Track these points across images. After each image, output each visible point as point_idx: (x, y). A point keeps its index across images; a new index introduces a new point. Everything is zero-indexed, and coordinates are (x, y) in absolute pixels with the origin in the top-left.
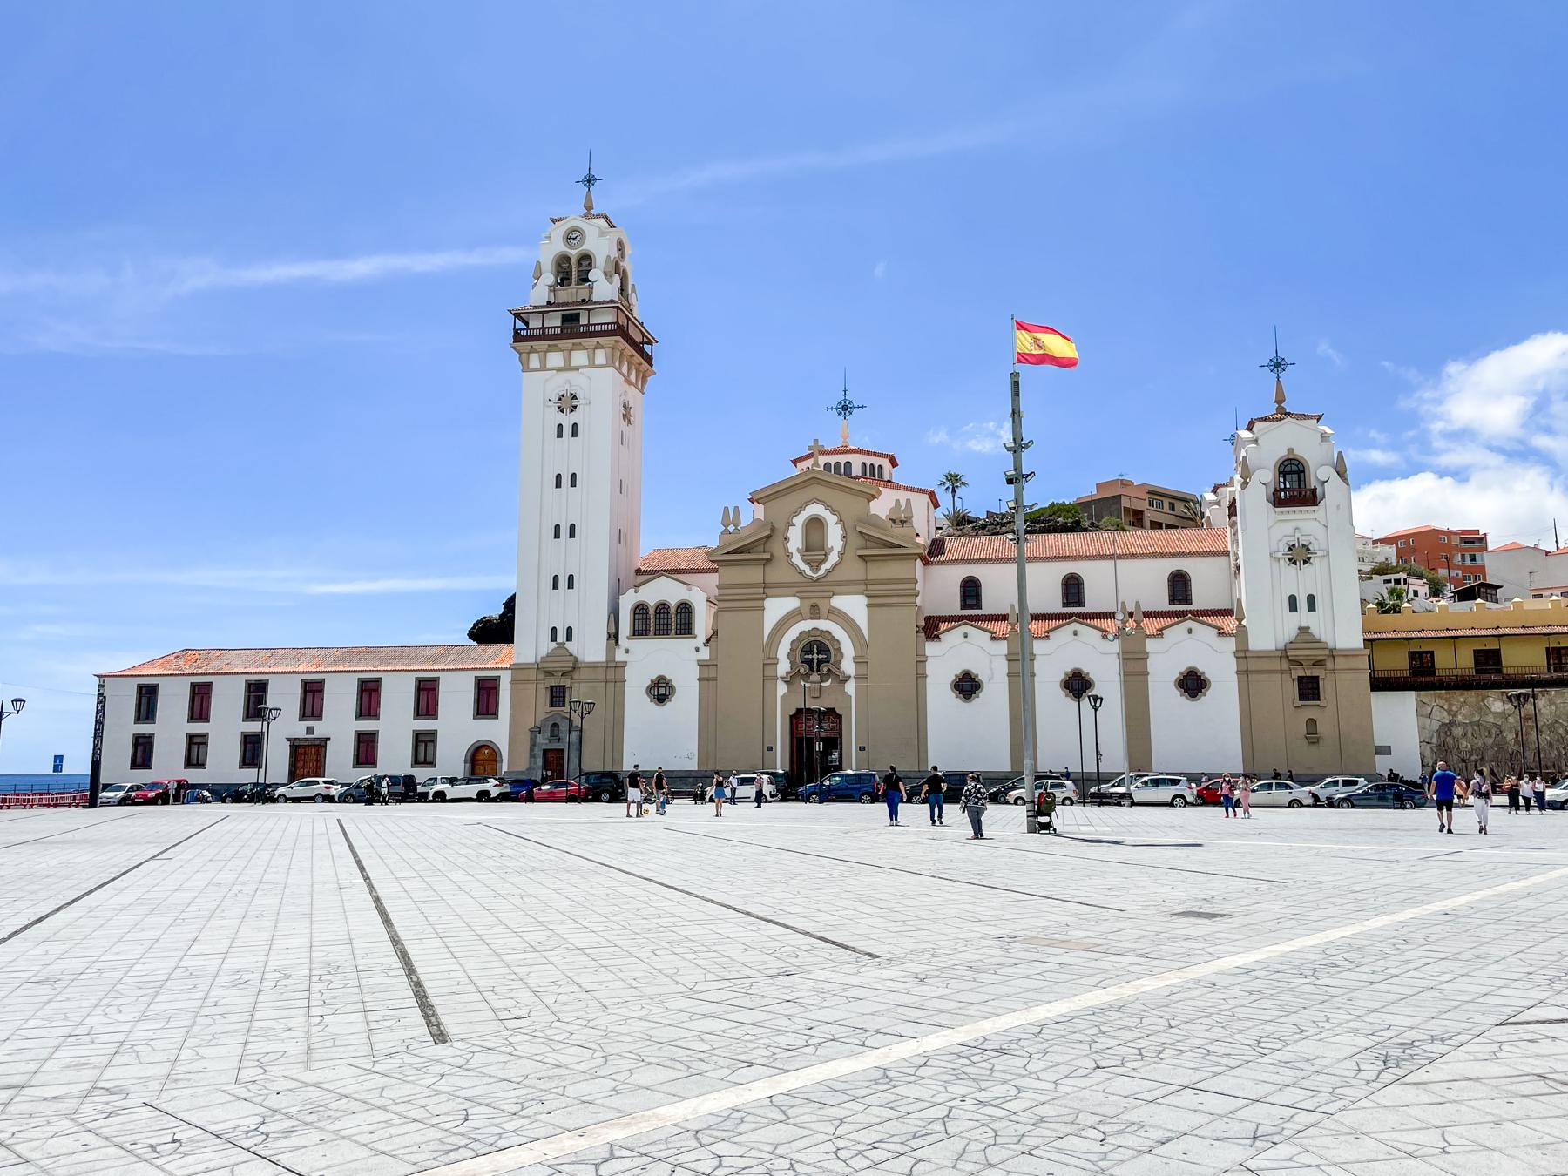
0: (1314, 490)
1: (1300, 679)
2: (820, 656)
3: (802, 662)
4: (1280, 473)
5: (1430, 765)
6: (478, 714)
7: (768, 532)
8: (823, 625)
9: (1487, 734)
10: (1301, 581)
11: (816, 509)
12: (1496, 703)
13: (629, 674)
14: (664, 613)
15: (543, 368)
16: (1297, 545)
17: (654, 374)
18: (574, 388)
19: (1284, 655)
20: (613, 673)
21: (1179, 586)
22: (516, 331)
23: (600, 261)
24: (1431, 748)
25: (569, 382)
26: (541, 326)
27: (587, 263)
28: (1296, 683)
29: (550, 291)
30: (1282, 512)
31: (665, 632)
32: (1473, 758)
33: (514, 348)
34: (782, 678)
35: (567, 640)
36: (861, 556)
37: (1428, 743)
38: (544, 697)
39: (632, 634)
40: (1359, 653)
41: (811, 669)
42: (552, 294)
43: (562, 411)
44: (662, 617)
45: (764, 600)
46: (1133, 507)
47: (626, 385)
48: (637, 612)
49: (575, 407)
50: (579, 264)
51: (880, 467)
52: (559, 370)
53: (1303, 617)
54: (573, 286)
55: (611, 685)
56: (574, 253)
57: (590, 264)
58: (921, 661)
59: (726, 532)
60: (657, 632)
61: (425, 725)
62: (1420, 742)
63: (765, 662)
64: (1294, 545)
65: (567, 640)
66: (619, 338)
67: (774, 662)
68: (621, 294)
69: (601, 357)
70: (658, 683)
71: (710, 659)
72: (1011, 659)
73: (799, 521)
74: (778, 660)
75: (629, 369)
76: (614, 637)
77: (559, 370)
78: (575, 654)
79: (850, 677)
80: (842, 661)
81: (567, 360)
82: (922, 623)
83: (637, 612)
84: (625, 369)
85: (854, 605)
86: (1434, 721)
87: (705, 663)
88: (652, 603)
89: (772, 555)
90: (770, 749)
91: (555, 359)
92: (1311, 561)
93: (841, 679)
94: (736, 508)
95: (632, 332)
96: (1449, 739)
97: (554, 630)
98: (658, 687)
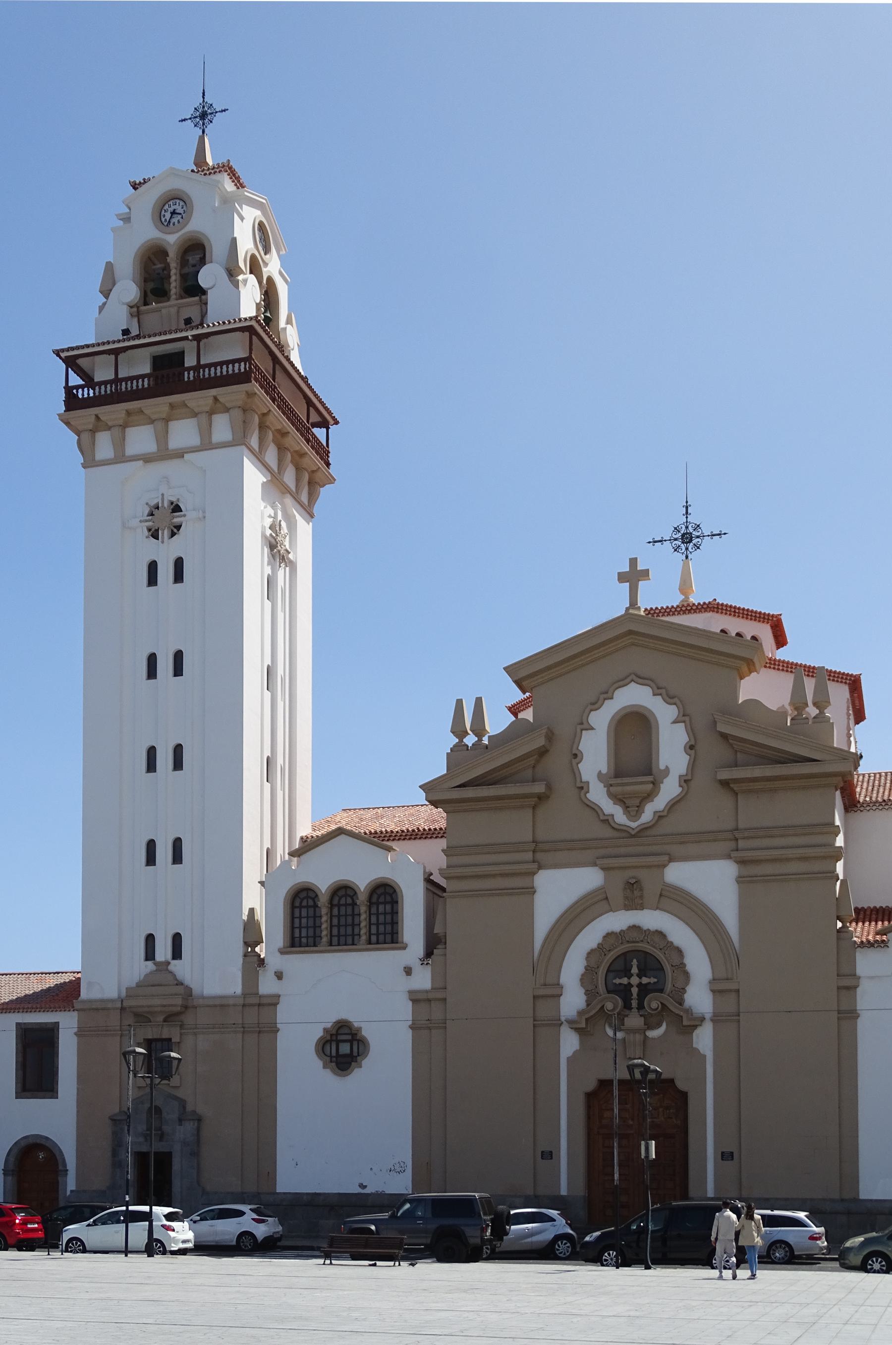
2: (645, 980)
3: (609, 992)
22: (69, 390)
26: (113, 377)
31: (350, 940)
34: (570, 1022)
41: (627, 1006)
42: (136, 320)
44: (343, 912)
45: (534, 874)
50: (183, 262)
54: (173, 302)
67: (555, 992)
69: (222, 427)
70: (337, 1034)
79: (703, 1019)
83: (297, 904)
88: (323, 884)
93: (685, 1023)
94: (479, 701)
98: (338, 1042)
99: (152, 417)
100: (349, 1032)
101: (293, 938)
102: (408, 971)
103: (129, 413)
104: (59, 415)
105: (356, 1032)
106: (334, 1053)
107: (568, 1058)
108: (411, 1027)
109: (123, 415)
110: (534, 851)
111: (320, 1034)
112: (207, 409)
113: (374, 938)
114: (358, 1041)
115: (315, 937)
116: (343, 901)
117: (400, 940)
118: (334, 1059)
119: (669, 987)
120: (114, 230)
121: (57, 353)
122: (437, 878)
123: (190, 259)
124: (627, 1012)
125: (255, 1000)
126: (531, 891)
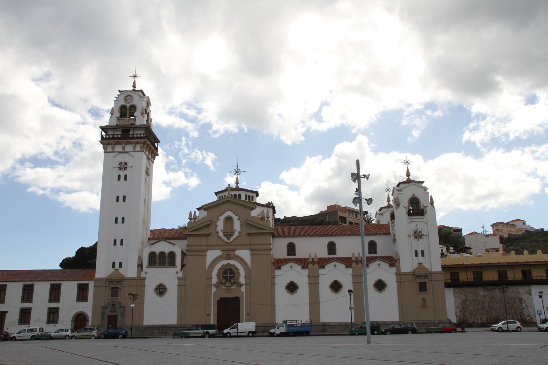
0: (423, 210)
1: (420, 283)
2: (231, 275)
3: (223, 278)
4: (410, 203)
5: (459, 316)
6: (78, 300)
7: (209, 223)
8: (232, 262)
9: (478, 304)
10: (420, 245)
11: (229, 214)
12: (481, 292)
13: (147, 283)
15: (113, 151)
16: (417, 231)
19: (415, 275)
20: (140, 282)
21: (372, 246)
22: (102, 135)
24: (459, 310)
25: (124, 158)
27: (134, 109)
28: (418, 284)
29: (117, 120)
30: (411, 218)
32: (474, 313)
34: (214, 285)
36: (248, 233)
37: (458, 307)
38: (109, 292)
39: (148, 265)
40: (441, 273)
41: (227, 281)
43: (121, 169)
45: (206, 251)
46: (343, 216)
49: (126, 168)
51: (252, 197)
52: (120, 152)
53: (421, 259)
54: (127, 118)
56: (128, 105)
57: (135, 109)
58: (273, 277)
60: (160, 264)
61: (54, 305)
62: (455, 307)
63: (207, 278)
64: (416, 231)
67: (211, 278)
69: (138, 148)
72: (309, 277)
73: (222, 218)
74: (212, 277)
76: (140, 266)
77: (120, 152)
79: (243, 284)
80: (240, 278)
81: (124, 148)
82: (273, 261)
85: (245, 254)
86: (460, 299)
87: (181, 278)
89: (210, 232)
90: (209, 315)
91: (119, 148)
92: (423, 237)
93: (239, 285)
96: (465, 306)
97: (114, 263)
98: (160, 288)
101: (149, 264)
104: (100, 141)
106: (159, 291)
107: (213, 293)
108: (178, 285)
111: (156, 287)
114: (165, 288)
116: (162, 256)
119: (236, 277)
120: (114, 101)
121: (100, 127)
122: (184, 251)
124: (226, 282)
125: (140, 279)
126: (206, 255)
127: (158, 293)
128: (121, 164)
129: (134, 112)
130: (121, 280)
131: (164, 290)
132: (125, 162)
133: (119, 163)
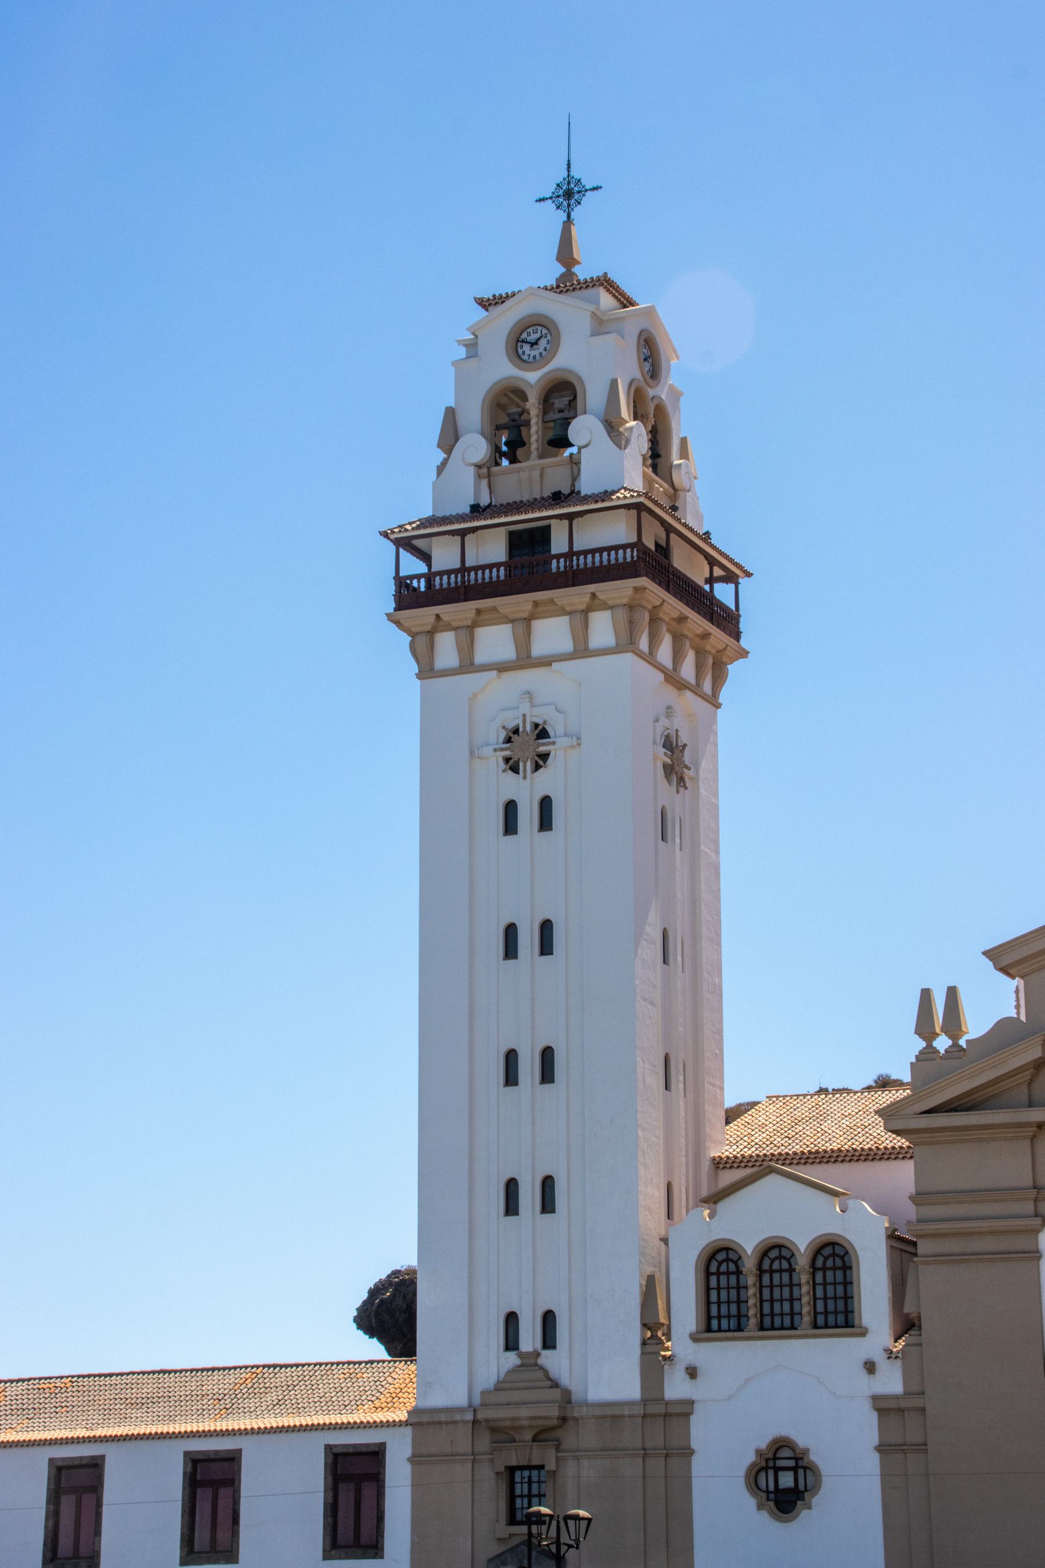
14: (781, 1271)
15: (467, 666)
17: (744, 654)
18: (537, 711)
23: (594, 396)
26: (458, 565)
27: (566, 400)
33: (398, 623)
35: (545, 1346)
39: (703, 1327)
42: (484, 483)
43: (515, 769)
47: (670, 692)
48: (713, 1268)
49: (545, 757)
52: (502, 668)
55: (656, 1465)
56: (533, 377)
59: (927, 1055)
65: (545, 1346)
66: (643, 581)
68: (655, 468)
70: (775, 1458)
71: (907, 1393)
75: (677, 656)
77: (502, 668)
78: (565, 1380)
81: (523, 641)
83: (713, 1268)
84: (665, 653)
87: (893, 1404)
88: (749, 1245)
94: (952, 993)
95: (682, 560)
97: (511, 1320)
98: (777, 1470)
99: (509, 616)
100: (792, 1455)
101: (709, 1318)
102: (870, 1367)
103: (479, 612)
104: (388, 615)
105: (801, 1456)
106: (772, 1487)
109: (473, 615)
110: (1036, 1200)
111: (751, 1458)
112: (583, 607)
113: (821, 1320)
114: (805, 1468)
115: (739, 1316)
116: (776, 1266)
117: (857, 1322)
118: (772, 1496)
123: (556, 401)
125: (662, 1410)
127: (768, 1499)
128: (515, 738)
129: (566, 422)
130: (555, 1422)
131: (801, 1480)
132: (536, 726)
133: (503, 735)
